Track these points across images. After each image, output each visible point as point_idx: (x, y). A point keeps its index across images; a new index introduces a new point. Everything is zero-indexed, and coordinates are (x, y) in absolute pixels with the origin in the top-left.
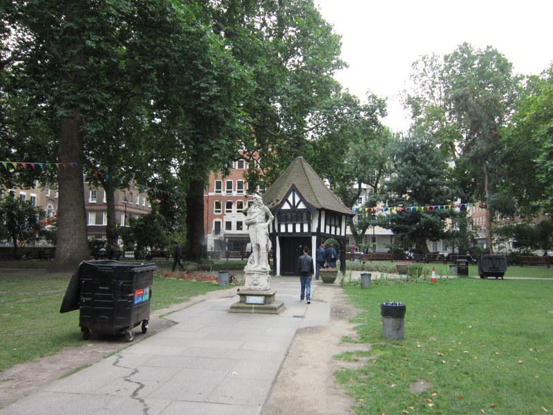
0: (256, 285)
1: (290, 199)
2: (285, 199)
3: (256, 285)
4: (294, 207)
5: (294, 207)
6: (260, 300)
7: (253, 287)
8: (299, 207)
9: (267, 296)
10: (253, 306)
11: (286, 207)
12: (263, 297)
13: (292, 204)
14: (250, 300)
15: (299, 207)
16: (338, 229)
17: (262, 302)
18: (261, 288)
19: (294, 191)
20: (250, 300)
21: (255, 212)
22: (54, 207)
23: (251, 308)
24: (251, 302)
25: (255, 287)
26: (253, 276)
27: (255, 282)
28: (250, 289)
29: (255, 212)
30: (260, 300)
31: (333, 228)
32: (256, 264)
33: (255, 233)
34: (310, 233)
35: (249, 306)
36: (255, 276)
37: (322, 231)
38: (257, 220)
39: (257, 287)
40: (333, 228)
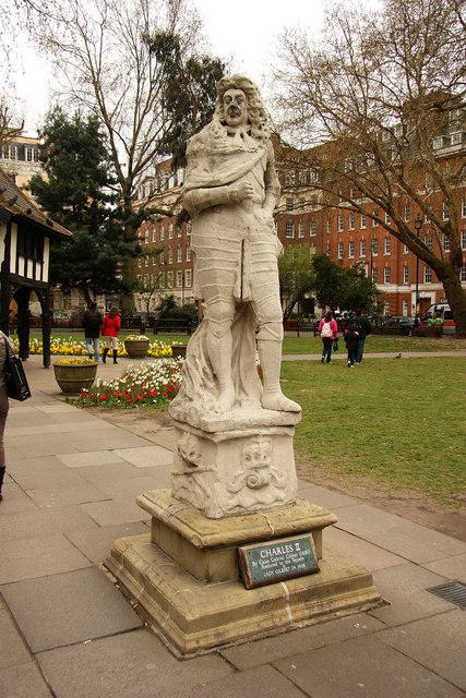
0: (258, 487)
7: (248, 499)
10: (285, 588)
16: (38, 267)
18: (282, 494)
21: (239, 152)
24: (269, 574)
26: (252, 448)
28: (240, 512)
29: (239, 152)
31: (30, 264)
32: (229, 391)
35: (269, 592)
37: (13, 270)
39: (267, 496)
40: (30, 264)
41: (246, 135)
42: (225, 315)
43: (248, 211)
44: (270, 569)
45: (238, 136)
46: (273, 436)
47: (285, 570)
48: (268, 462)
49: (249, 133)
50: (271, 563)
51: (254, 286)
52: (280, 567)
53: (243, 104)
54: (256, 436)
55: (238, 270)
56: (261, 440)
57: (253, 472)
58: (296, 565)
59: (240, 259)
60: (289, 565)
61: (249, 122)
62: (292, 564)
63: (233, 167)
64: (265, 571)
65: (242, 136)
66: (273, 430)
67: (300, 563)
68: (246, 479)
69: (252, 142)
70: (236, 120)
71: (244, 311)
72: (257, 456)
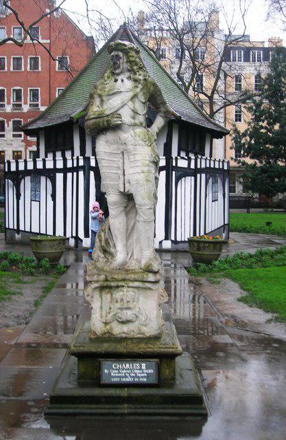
6: (140, 372)
7: (118, 330)
9: (165, 359)
14: (118, 372)
17: (153, 380)
18: (145, 329)
20: (118, 372)
25: (125, 328)
27: (128, 314)
28: (108, 337)
30: (140, 372)
33: (118, 159)
36: (126, 294)
38: (126, 116)
41: (125, 80)
42: (115, 203)
43: (125, 132)
44: (117, 377)
45: (119, 81)
46: (137, 288)
47: (129, 380)
48: (131, 305)
49: (129, 78)
50: (119, 373)
51: (132, 182)
52: (126, 377)
53: (121, 61)
54: (123, 286)
55: (120, 172)
56: (125, 290)
57: (119, 311)
58: (138, 377)
59: (121, 165)
60: (134, 377)
61: (129, 71)
62: (136, 376)
63: (115, 102)
64: (114, 377)
65: (122, 81)
66: (136, 284)
67: (142, 377)
68: (115, 315)
69: (129, 84)
70: (117, 71)
71: (129, 198)
72: (122, 300)
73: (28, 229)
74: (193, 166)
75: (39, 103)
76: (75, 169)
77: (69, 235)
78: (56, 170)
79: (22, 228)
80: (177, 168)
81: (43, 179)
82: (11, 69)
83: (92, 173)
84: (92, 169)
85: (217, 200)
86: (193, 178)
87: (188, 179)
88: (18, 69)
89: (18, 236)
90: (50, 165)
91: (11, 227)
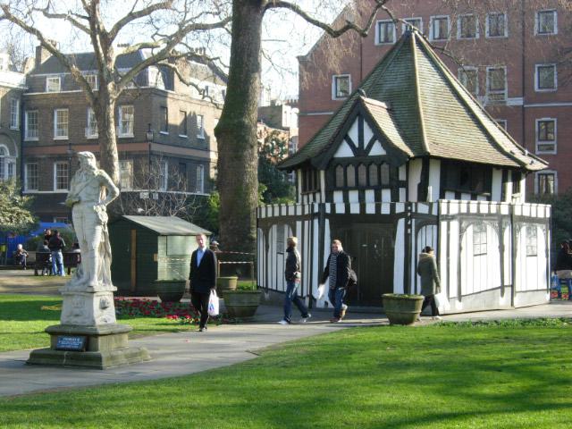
0: (77, 315)
1: (354, 134)
2: (343, 135)
3: (77, 315)
4: (361, 152)
5: (361, 152)
8: (371, 154)
10: (66, 353)
11: (345, 152)
12: (83, 338)
13: (357, 145)
15: (372, 153)
19: (359, 114)
22: (12, 153)
23: (62, 357)
34: (393, 217)
47: (69, 347)
48: (79, 305)
73: (274, 288)
74: (434, 212)
75: (506, 92)
76: (312, 216)
77: (305, 294)
78: (296, 218)
79: (270, 287)
80: (416, 215)
81: (286, 227)
82: (487, 35)
83: (327, 221)
84: (327, 216)
85: (536, 256)
86: (435, 227)
87: (429, 227)
88: (469, 36)
89: (267, 296)
90: (291, 213)
91: (261, 285)
